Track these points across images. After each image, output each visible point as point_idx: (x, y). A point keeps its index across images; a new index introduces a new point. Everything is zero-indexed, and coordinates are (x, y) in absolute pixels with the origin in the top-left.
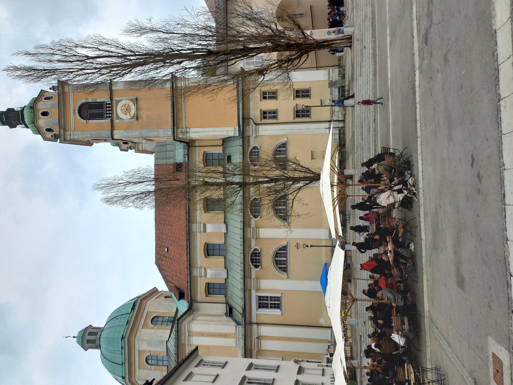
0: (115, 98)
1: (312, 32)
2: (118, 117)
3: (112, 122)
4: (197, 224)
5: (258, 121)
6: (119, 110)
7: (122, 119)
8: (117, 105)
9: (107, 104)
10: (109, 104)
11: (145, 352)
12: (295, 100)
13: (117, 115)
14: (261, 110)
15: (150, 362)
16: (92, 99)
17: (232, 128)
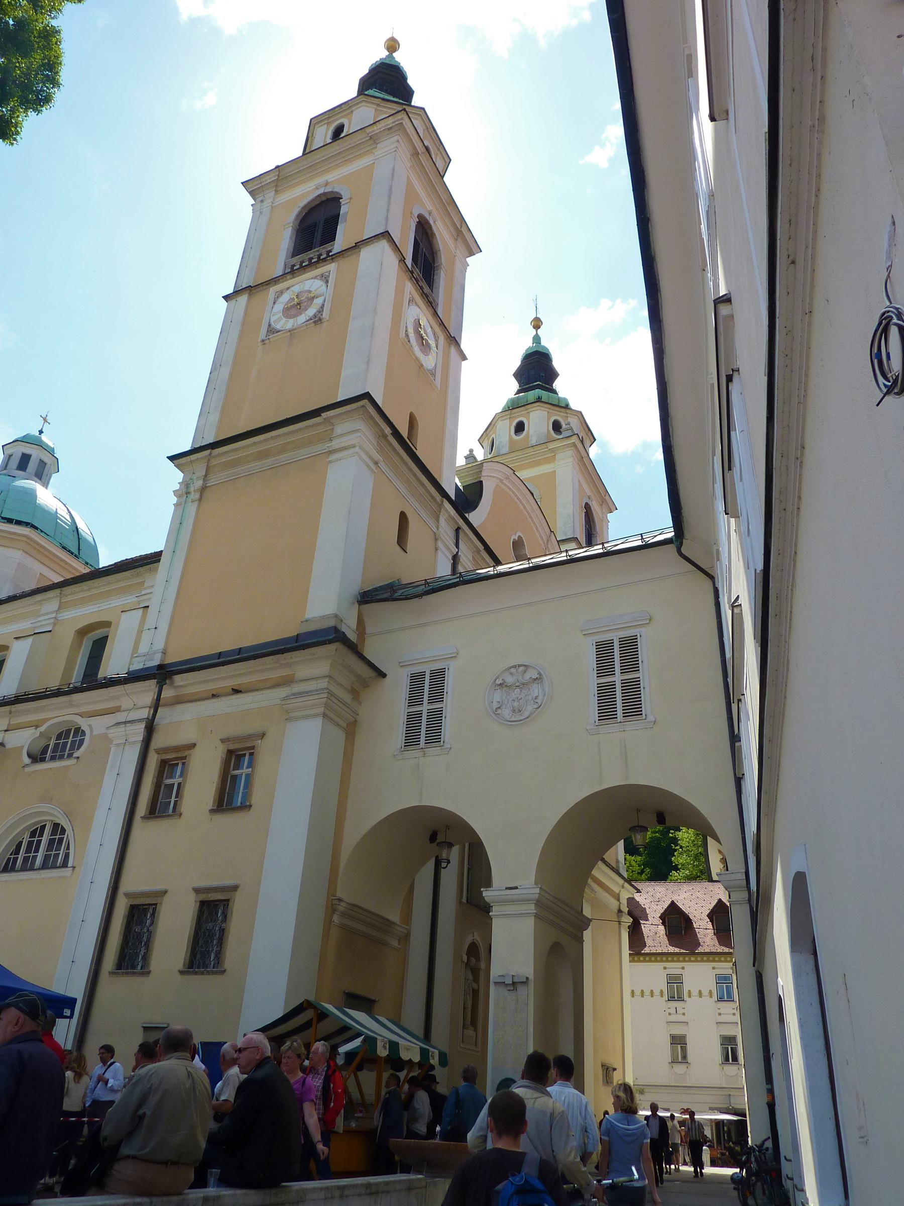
0: (331, 268)
1: (522, 990)
5: (158, 742)
7: (274, 303)
8: (315, 278)
12: (193, 894)
13: (288, 288)
14: (194, 745)
16: (346, 213)
17: (160, 645)
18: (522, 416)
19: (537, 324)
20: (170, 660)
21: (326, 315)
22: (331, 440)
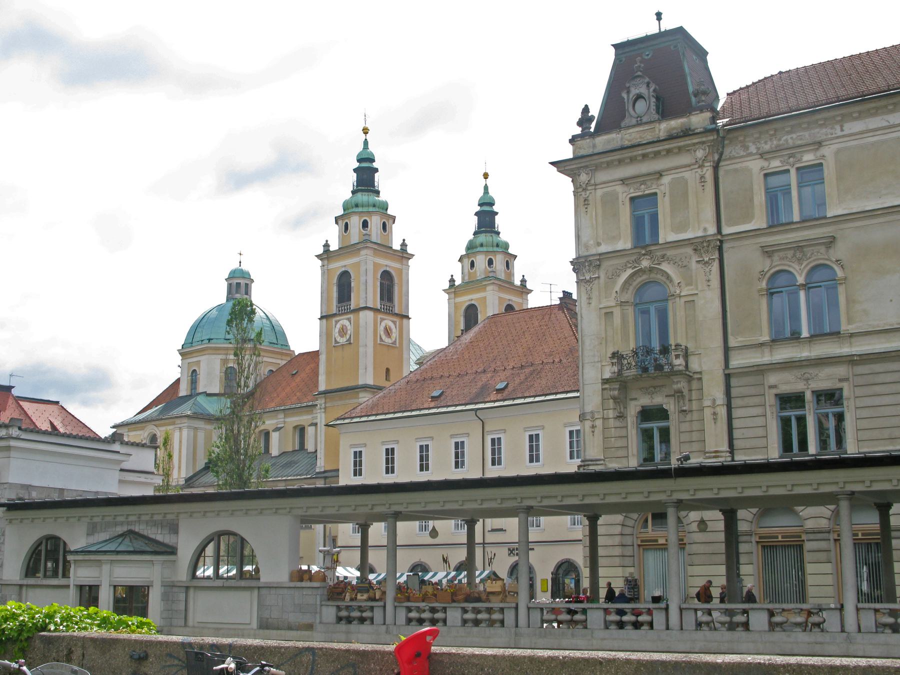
0: (351, 316)
2: (337, 322)
3: (334, 315)
4: (283, 420)
6: (344, 321)
9: (350, 305)
10: (350, 308)
11: (199, 367)
13: (339, 321)
15: (194, 375)
18: (473, 257)
19: (486, 176)
20: (326, 469)
21: (352, 342)
22: (358, 398)
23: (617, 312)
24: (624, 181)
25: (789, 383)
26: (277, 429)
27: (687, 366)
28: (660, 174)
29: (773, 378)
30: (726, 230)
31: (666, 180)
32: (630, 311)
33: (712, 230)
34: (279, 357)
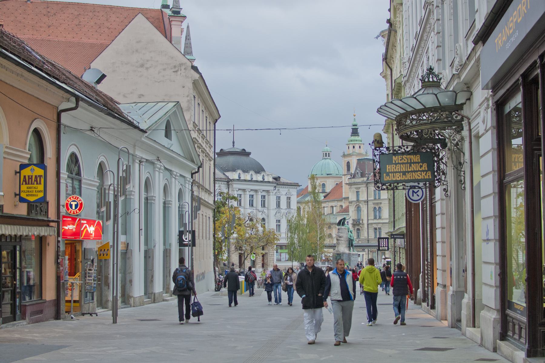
23: (354, 211)
24: (355, 188)
25: (375, 226)
26: (336, 206)
27: (362, 222)
28: (360, 188)
29: (373, 225)
30: (369, 199)
31: (361, 189)
32: (356, 211)
33: (366, 199)
34: (340, 178)
